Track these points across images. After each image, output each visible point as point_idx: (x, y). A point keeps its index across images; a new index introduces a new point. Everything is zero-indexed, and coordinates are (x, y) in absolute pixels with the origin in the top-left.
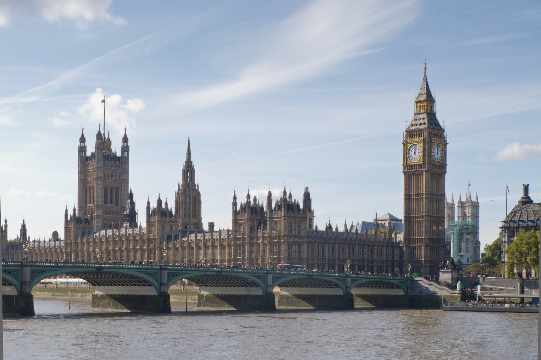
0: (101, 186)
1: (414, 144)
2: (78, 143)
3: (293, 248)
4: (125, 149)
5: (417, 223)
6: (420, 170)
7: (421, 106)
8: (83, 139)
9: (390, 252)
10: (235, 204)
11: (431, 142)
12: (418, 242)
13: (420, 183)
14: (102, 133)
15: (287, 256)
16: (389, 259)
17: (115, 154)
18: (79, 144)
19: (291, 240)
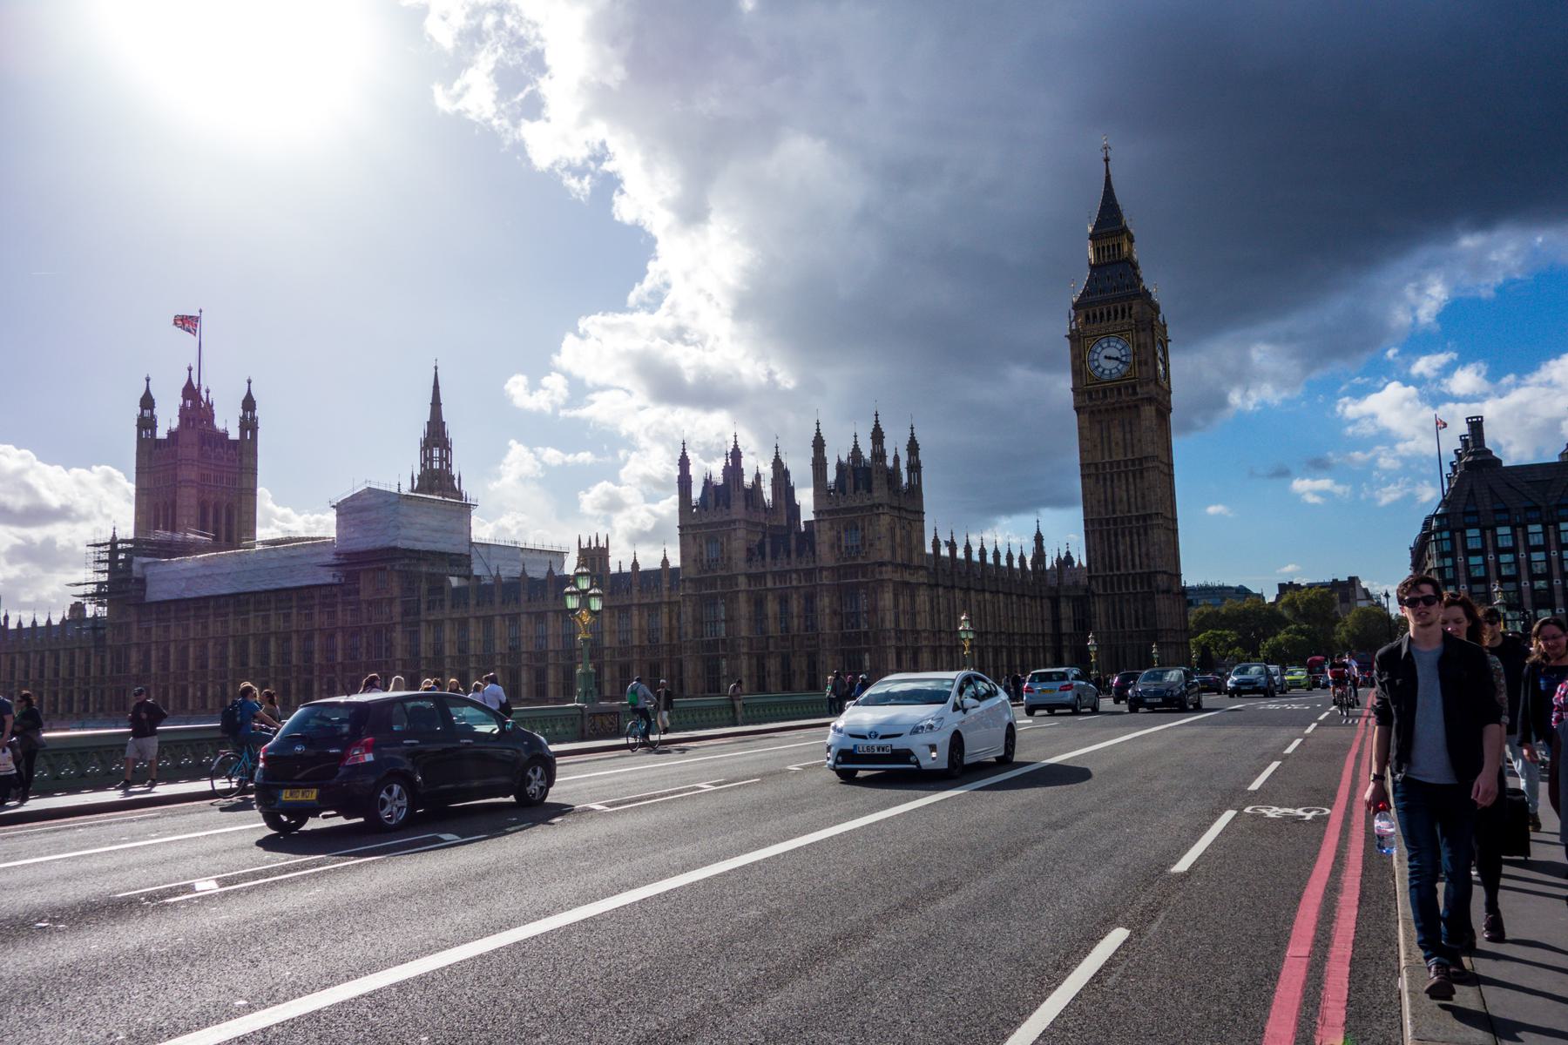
0: (194, 502)
1: (1107, 335)
2: (137, 410)
3: (901, 601)
4: (249, 424)
5: (1127, 533)
6: (1127, 399)
7: (1114, 246)
8: (147, 402)
9: (1048, 614)
10: (685, 482)
11: (1152, 330)
12: (1134, 582)
13: (1131, 432)
14: (195, 383)
15: (893, 626)
16: (1046, 631)
17: (226, 434)
18: (139, 412)
19: (897, 577)
